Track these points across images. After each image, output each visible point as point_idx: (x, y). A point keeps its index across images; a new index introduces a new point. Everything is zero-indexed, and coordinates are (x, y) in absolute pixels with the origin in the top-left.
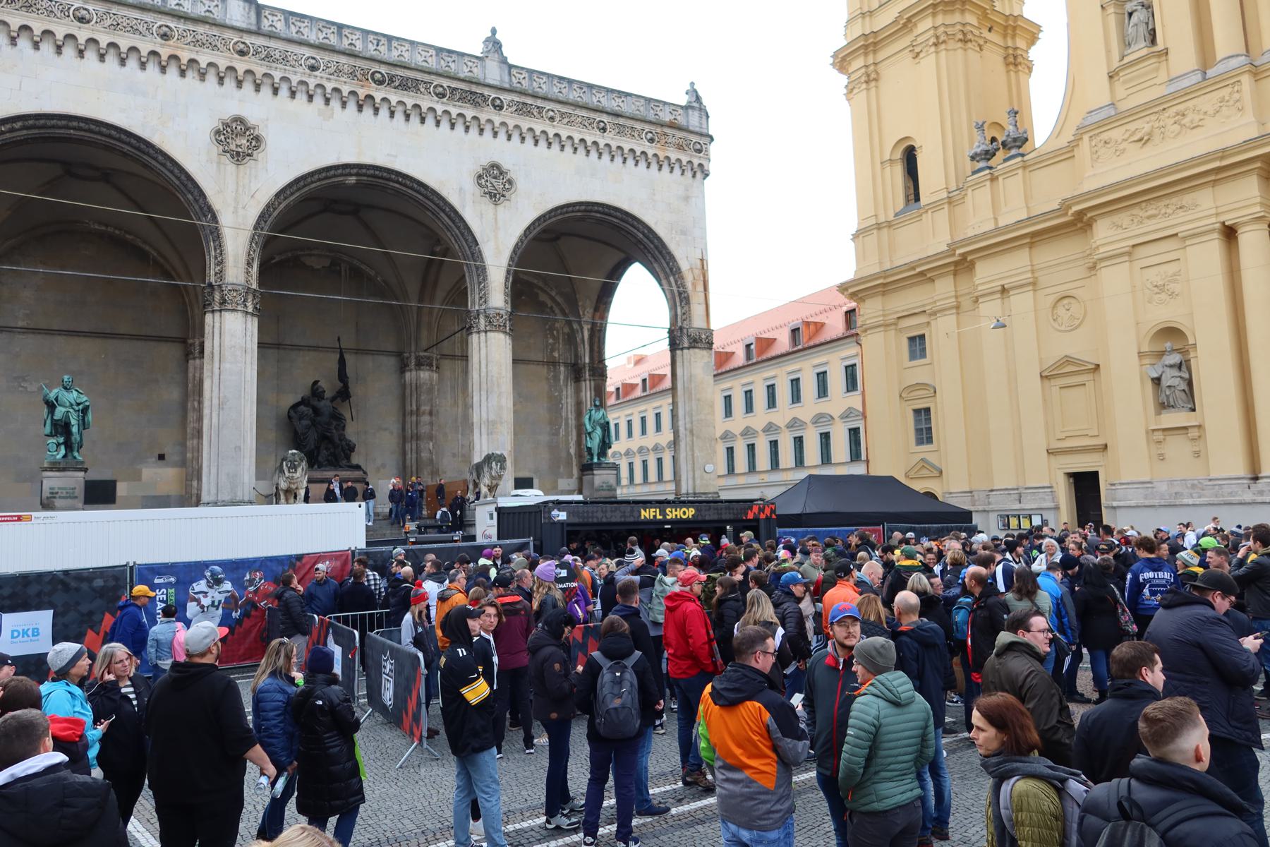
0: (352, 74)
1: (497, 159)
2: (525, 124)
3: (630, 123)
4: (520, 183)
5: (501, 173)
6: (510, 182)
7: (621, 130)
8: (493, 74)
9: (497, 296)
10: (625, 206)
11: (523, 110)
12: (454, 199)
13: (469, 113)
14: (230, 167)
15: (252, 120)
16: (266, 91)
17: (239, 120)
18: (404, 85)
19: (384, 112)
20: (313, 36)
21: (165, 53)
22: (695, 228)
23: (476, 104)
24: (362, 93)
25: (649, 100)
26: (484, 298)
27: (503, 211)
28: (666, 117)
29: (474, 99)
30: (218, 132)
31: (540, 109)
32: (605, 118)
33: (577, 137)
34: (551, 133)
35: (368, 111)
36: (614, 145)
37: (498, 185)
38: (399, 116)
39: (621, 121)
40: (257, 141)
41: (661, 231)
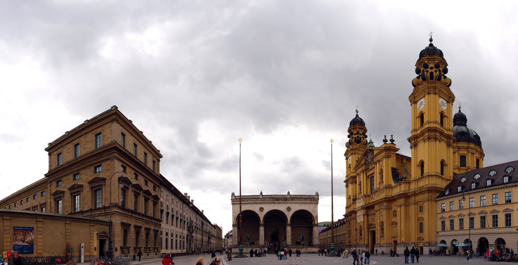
0: (272, 200)
1: (289, 206)
2: (292, 202)
3: (307, 199)
4: (292, 209)
5: (290, 208)
6: (291, 209)
7: (305, 200)
8: (288, 197)
9: (289, 222)
10: (306, 210)
11: (292, 200)
12: (284, 212)
13: (285, 202)
14: (261, 212)
15: (263, 207)
16: (264, 204)
17: (262, 207)
18: (278, 200)
19: (276, 204)
20: (268, 197)
21: (254, 202)
22: (316, 211)
23: (286, 201)
24: (273, 202)
25: (309, 195)
26: (288, 223)
27: (290, 212)
28: (312, 197)
29: (286, 200)
30: (260, 209)
31: (294, 200)
32: (303, 199)
33: (299, 202)
34: (296, 202)
35: (274, 204)
36: (304, 202)
37: (289, 209)
38: (278, 204)
39: (305, 199)
40: (263, 209)
41: (311, 212)
